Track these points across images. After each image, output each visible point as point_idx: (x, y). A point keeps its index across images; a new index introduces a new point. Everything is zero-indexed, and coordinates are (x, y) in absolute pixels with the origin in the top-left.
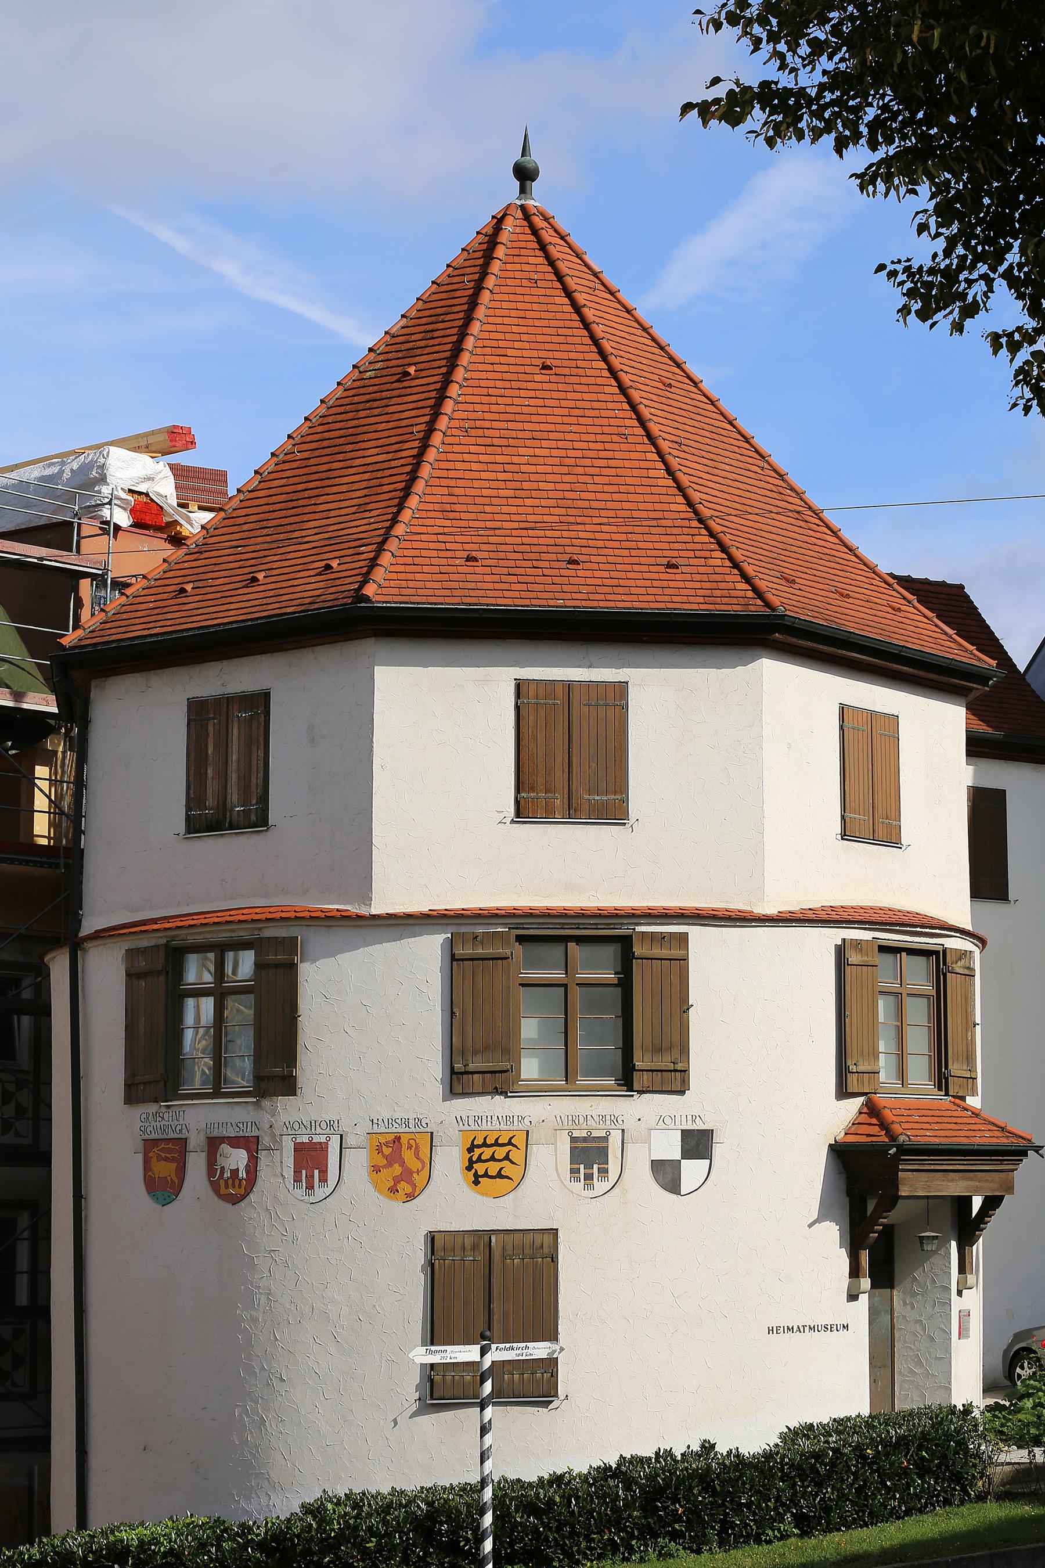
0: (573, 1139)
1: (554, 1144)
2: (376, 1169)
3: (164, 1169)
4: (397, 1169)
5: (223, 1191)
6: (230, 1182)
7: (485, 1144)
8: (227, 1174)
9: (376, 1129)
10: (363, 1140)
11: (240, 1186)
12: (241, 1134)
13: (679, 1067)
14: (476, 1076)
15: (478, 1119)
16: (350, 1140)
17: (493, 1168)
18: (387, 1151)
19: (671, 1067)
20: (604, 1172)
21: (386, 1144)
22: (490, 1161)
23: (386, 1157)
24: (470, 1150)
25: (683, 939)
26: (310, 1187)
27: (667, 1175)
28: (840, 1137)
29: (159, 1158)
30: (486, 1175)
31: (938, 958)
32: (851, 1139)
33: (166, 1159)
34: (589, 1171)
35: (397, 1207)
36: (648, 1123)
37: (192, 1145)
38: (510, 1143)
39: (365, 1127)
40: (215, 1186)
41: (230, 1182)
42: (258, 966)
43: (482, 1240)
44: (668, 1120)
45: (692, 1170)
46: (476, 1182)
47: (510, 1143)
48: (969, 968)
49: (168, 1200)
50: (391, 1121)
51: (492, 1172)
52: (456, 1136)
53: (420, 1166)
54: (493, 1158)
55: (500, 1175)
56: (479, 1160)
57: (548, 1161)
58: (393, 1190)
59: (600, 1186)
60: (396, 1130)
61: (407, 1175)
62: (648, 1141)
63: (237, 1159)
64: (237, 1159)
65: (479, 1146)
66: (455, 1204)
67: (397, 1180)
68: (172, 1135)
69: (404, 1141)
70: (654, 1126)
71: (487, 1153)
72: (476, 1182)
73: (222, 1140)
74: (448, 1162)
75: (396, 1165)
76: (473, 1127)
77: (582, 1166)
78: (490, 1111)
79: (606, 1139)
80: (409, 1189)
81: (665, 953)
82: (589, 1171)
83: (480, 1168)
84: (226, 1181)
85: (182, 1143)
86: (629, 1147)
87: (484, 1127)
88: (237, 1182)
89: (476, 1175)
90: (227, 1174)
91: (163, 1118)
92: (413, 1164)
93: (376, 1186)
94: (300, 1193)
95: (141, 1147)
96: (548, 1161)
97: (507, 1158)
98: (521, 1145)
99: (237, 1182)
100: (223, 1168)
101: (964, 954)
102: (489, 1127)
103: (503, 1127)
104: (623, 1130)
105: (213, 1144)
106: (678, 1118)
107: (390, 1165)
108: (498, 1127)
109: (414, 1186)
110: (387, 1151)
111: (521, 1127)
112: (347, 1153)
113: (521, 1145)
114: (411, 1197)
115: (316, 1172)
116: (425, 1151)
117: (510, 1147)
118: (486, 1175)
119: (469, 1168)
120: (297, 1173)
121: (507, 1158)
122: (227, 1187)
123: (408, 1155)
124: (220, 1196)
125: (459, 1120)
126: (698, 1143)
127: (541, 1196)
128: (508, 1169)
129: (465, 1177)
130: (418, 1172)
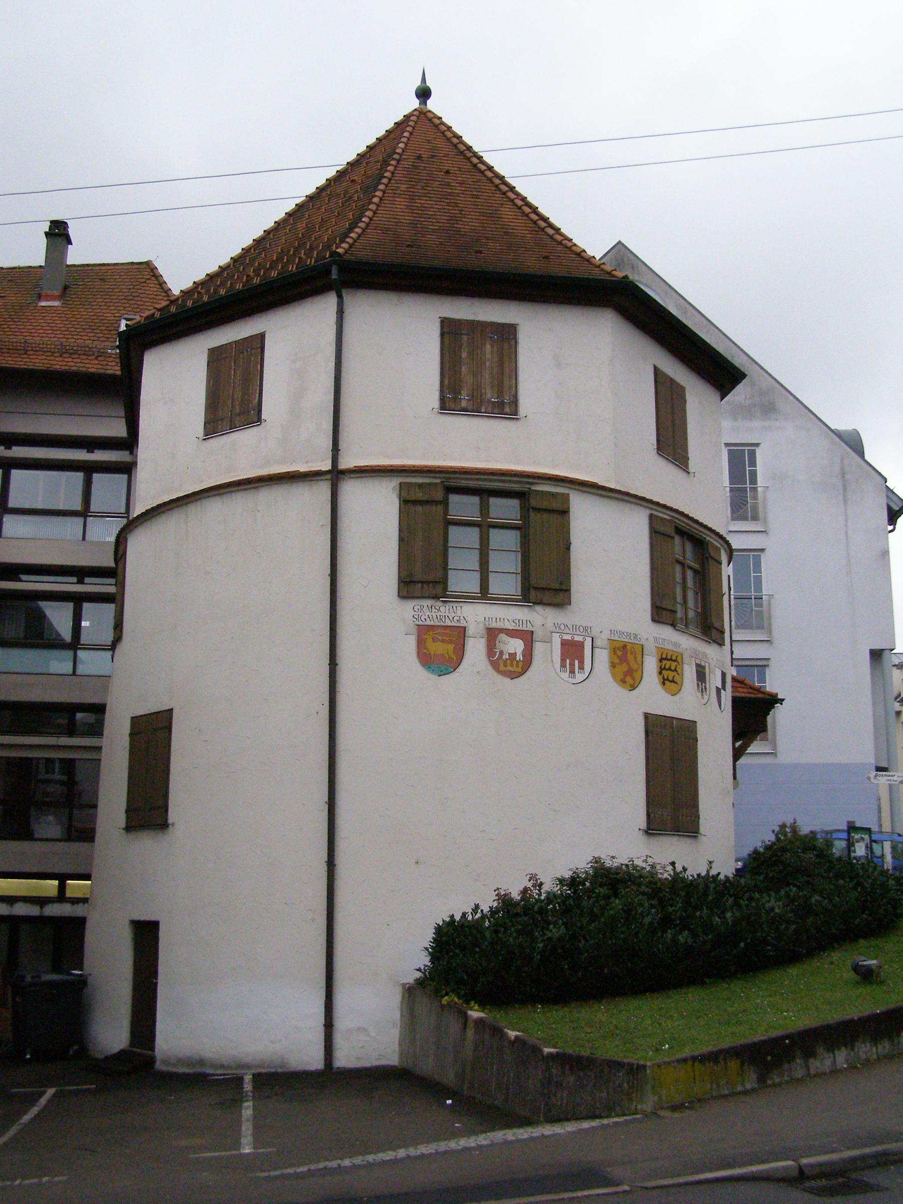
2: (613, 665)
4: (624, 668)
5: (502, 668)
6: (509, 661)
11: (517, 665)
12: (517, 628)
23: (618, 657)
26: (572, 672)
29: (434, 640)
33: (443, 641)
37: (470, 632)
39: (606, 635)
40: (495, 665)
49: (446, 672)
52: (654, 650)
54: (670, 669)
55: (673, 681)
56: (665, 669)
58: (623, 681)
61: (630, 672)
63: (516, 646)
64: (516, 646)
68: (449, 624)
73: (501, 631)
84: (505, 662)
88: (515, 663)
91: (439, 610)
95: (414, 630)
99: (515, 663)
100: (501, 653)
105: (492, 634)
107: (621, 663)
112: (597, 651)
114: (633, 688)
115: (576, 662)
116: (639, 657)
118: (668, 679)
119: (660, 673)
121: (675, 670)
123: (630, 657)
124: (498, 671)
125: (655, 639)
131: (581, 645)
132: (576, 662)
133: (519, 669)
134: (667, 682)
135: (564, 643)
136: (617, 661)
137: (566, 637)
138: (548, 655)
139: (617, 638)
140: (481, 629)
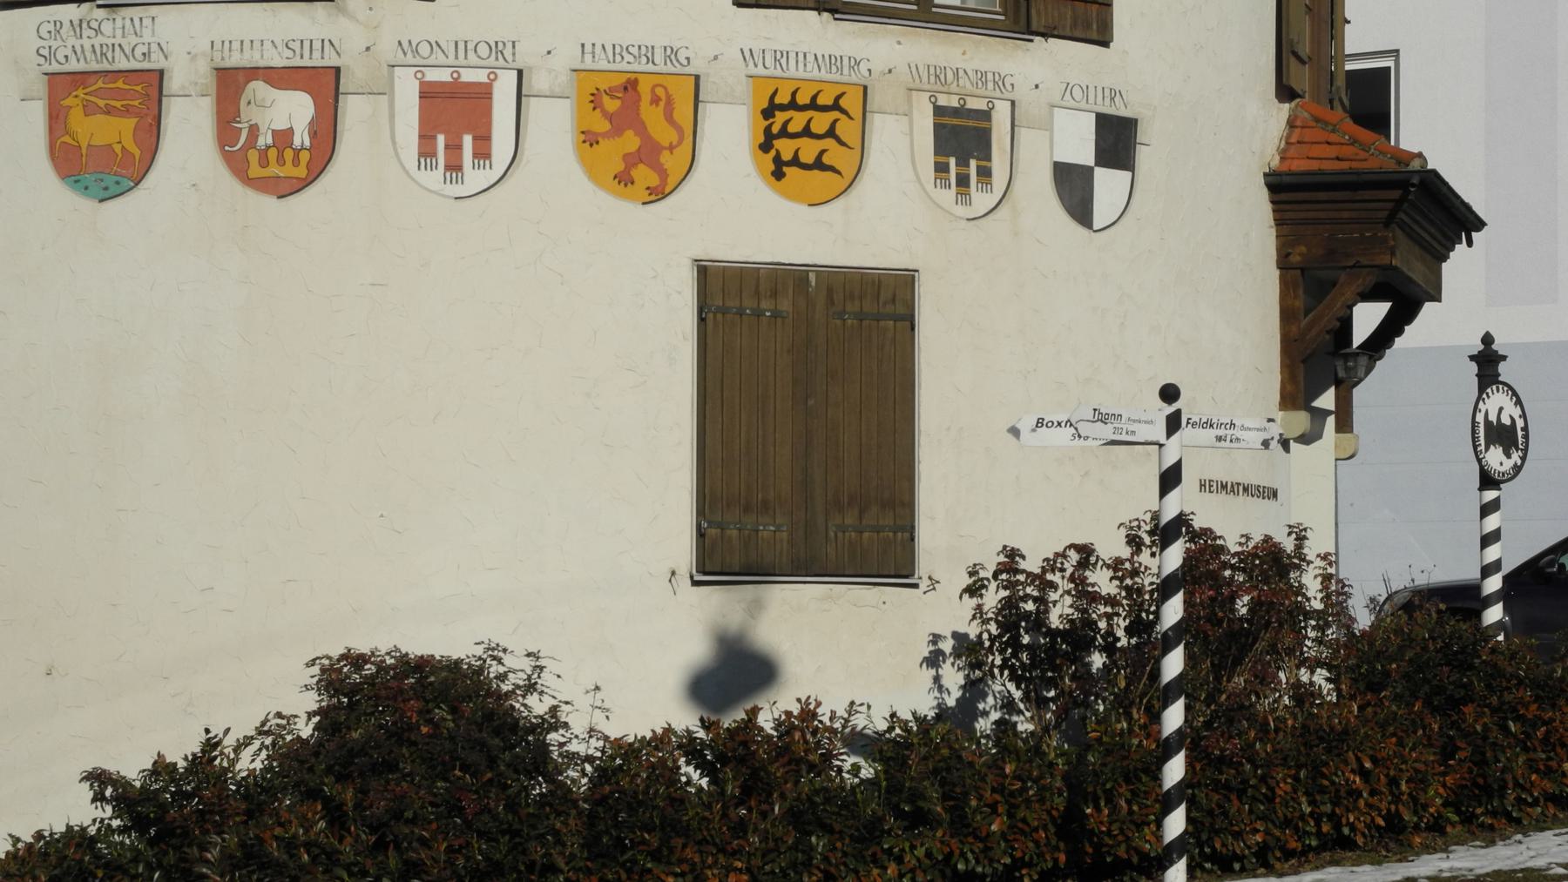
0: (939, 111)
2: (589, 139)
4: (631, 142)
5: (255, 171)
6: (273, 153)
7: (793, 105)
8: (265, 139)
9: (588, 63)
10: (564, 79)
11: (296, 162)
12: (297, 62)
15: (780, 56)
16: (537, 82)
18: (612, 105)
21: (610, 93)
22: (803, 136)
23: (610, 117)
24: (768, 113)
26: (454, 167)
27: (1073, 188)
28: (1276, 163)
29: (89, 109)
30: (795, 162)
32: (1285, 168)
33: (109, 111)
34: (963, 170)
35: (628, 213)
37: (173, 83)
38: (836, 106)
39: (567, 56)
40: (237, 164)
41: (273, 153)
44: (1077, 93)
45: (1109, 186)
46: (778, 174)
47: (836, 106)
49: (114, 190)
50: (618, 51)
51: (807, 157)
52: (742, 88)
53: (674, 138)
54: (806, 132)
55: (819, 165)
56: (784, 133)
57: (899, 144)
58: (624, 179)
59: (981, 200)
60: (624, 66)
61: (649, 153)
62: (1049, 126)
63: (291, 111)
64: (291, 111)
65: (783, 108)
66: (740, 213)
67: (631, 160)
68: (123, 64)
69: (644, 89)
71: (798, 121)
72: (778, 174)
73: (253, 73)
74: (728, 132)
75: (629, 134)
76: (771, 72)
77: (952, 161)
79: (986, 115)
80: (654, 180)
82: (963, 170)
83: (786, 148)
84: (264, 153)
86: (1023, 134)
87: (792, 72)
88: (289, 154)
89: (778, 161)
90: (265, 139)
91: (98, 31)
92: (662, 132)
94: (434, 177)
95: (40, 87)
96: (899, 144)
97: (831, 133)
98: (856, 111)
99: (289, 154)
100: (254, 130)
102: (801, 74)
103: (824, 75)
104: (1013, 103)
105: (230, 84)
106: (1092, 90)
107: (617, 131)
108: (815, 74)
109: (663, 174)
110: (612, 105)
111: (854, 79)
112: (533, 106)
113: (855, 110)
114: (658, 194)
115: (468, 140)
116: (683, 112)
117: (835, 114)
118: (795, 162)
119: (766, 147)
121: (831, 133)
122: (264, 163)
123: (652, 116)
124: (248, 181)
125: (747, 55)
126: (1117, 140)
130: (671, 148)
131: (481, 95)
132: (468, 140)
133: (301, 172)
134: (790, 171)
135: (429, 94)
136: (604, 126)
137: (433, 75)
138: (378, 129)
139: (603, 65)
140: (202, 73)
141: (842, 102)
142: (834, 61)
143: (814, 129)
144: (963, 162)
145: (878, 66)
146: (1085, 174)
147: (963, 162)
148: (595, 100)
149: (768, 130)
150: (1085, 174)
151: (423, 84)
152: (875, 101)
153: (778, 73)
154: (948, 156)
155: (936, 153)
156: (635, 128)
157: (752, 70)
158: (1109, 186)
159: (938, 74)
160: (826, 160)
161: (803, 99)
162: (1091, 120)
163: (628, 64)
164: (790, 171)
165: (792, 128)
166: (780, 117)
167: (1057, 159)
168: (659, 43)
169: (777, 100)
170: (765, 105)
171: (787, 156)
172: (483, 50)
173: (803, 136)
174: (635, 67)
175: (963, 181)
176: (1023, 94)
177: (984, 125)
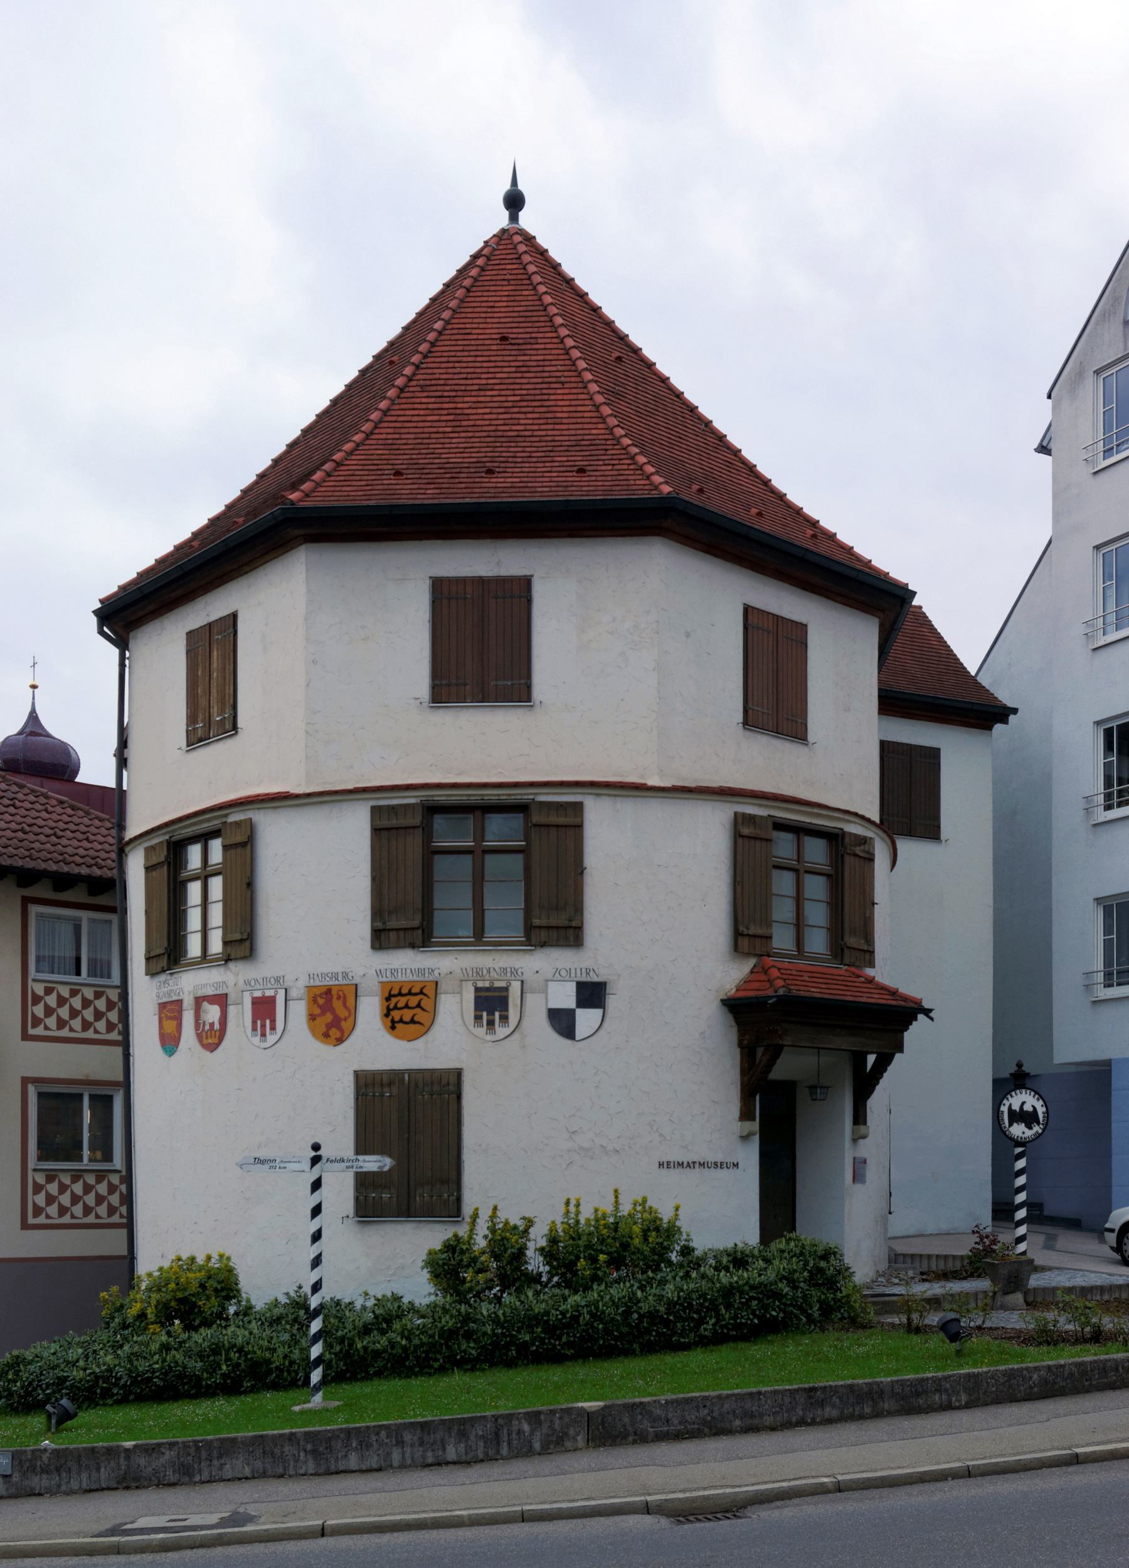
0: (477, 990)
1: (460, 993)
2: (312, 1017)
3: (170, 1026)
4: (329, 1017)
5: (205, 1041)
7: (400, 994)
8: (207, 1027)
9: (312, 983)
13: (574, 924)
14: (391, 934)
15: (393, 972)
16: (293, 993)
17: (407, 1015)
19: (566, 923)
20: (504, 1019)
21: (321, 996)
22: (407, 1008)
23: (320, 1007)
24: (388, 999)
25: (578, 807)
26: (263, 1035)
27: (563, 1022)
30: (401, 1021)
31: (834, 838)
32: (741, 994)
34: (491, 1017)
36: (545, 977)
37: (185, 1005)
38: (421, 993)
39: (303, 982)
40: (200, 1037)
42: (225, 848)
43: (393, 1078)
44: (563, 973)
45: (587, 1019)
46: (393, 1028)
47: (421, 993)
48: (868, 852)
50: (324, 975)
51: (407, 1018)
52: (377, 988)
53: (346, 1014)
54: (407, 1006)
55: (413, 1021)
56: (396, 1008)
57: (454, 1010)
58: (326, 1035)
59: (501, 1031)
60: (326, 983)
61: (336, 1023)
62: (545, 991)
63: (212, 1013)
65: (395, 996)
66: (374, 1047)
67: (329, 1026)
69: (334, 992)
70: (550, 977)
71: (402, 1001)
72: (393, 1028)
74: (370, 1009)
75: (328, 1014)
76: (390, 979)
77: (485, 1014)
78: (406, 964)
79: (506, 989)
80: (338, 1035)
81: (562, 820)
82: (491, 1017)
83: (397, 1015)
85: (180, 1002)
86: (529, 997)
89: (393, 1021)
90: (207, 1027)
92: (341, 1012)
93: (313, 1031)
96: (454, 1010)
97: (419, 1006)
101: (864, 841)
102: (404, 979)
103: (415, 978)
104: (522, 982)
107: (323, 1013)
109: (342, 1032)
110: (321, 1001)
111: (431, 978)
112: (291, 1004)
113: (431, 994)
114: (340, 1041)
115: (268, 1022)
116: (350, 1002)
117: (421, 996)
119: (387, 1015)
120: (254, 1023)
121: (419, 1006)
123: (337, 1004)
125: (379, 973)
126: (592, 994)
127: (447, 1040)
128: (420, 1016)
129: (384, 1024)
130: (345, 1019)
131: (272, 1001)
133: (216, 1041)
134: (399, 1026)
135: (256, 1002)
139: (318, 983)
141: (424, 991)
142: (421, 971)
143: (410, 1005)
144: (491, 1013)
145: (444, 971)
146: (570, 1013)
147: (491, 1013)
148: (314, 1000)
149: (388, 1007)
150: (570, 1013)
151: (253, 998)
152: (442, 987)
153: (393, 979)
154: (482, 1011)
155: (476, 1010)
156: (331, 1011)
157: (381, 979)
158: (587, 1019)
159: (478, 972)
160: (416, 1019)
161: (405, 991)
162: (574, 984)
163: (328, 982)
164: (399, 1026)
165: (399, 1005)
166: (394, 1000)
167: (552, 1005)
168: (340, 970)
169: (393, 992)
170: (387, 995)
171: (397, 1019)
172: (273, 981)
173: (407, 1008)
174: (331, 983)
175: (491, 1023)
176: (529, 976)
177: (504, 994)
